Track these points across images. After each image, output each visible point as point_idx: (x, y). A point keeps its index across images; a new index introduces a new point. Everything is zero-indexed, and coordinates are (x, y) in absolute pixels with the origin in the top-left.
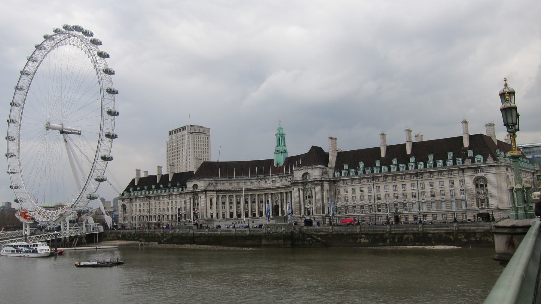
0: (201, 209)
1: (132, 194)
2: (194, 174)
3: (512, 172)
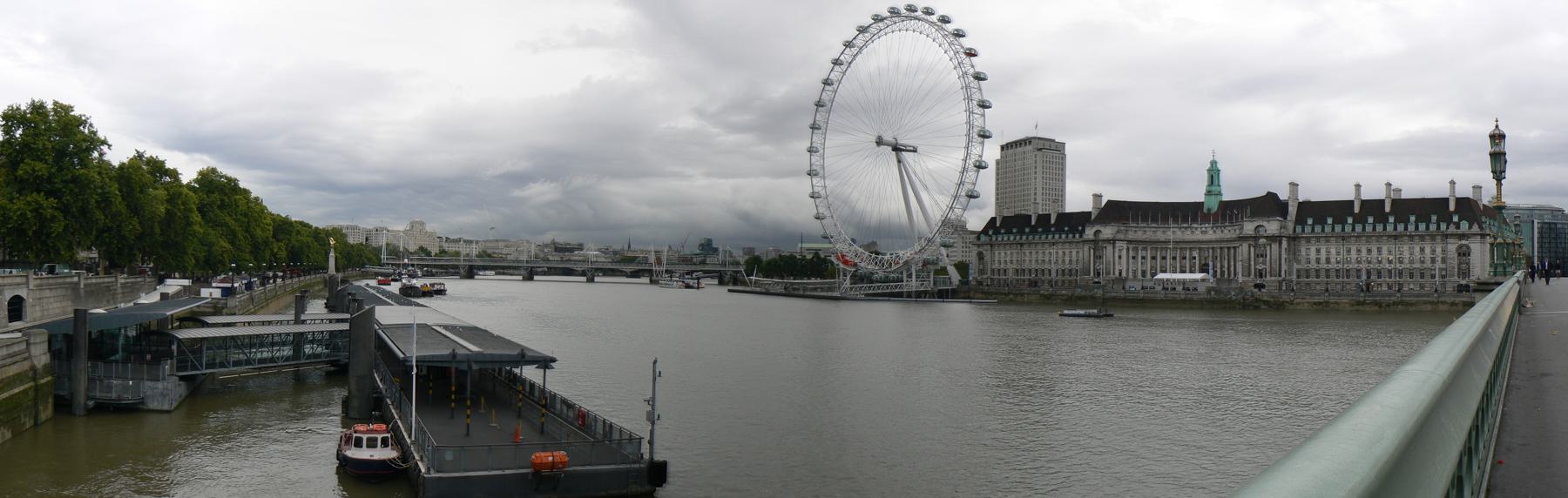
1: (994, 239)
2: (1093, 217)
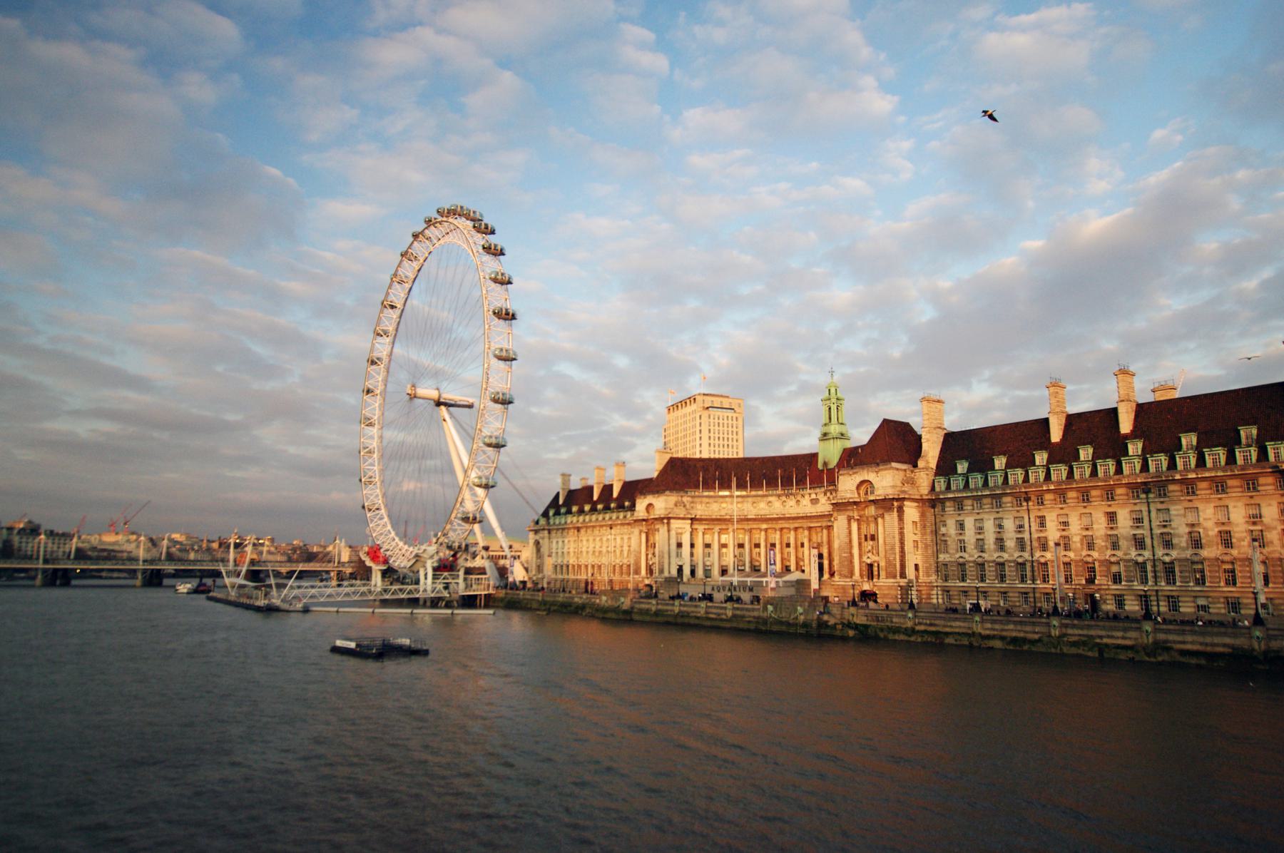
0: (659, 556)
1: (551, 521)
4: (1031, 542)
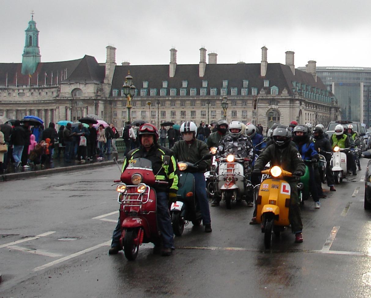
3: (306, 106)
4: (158, 123)
